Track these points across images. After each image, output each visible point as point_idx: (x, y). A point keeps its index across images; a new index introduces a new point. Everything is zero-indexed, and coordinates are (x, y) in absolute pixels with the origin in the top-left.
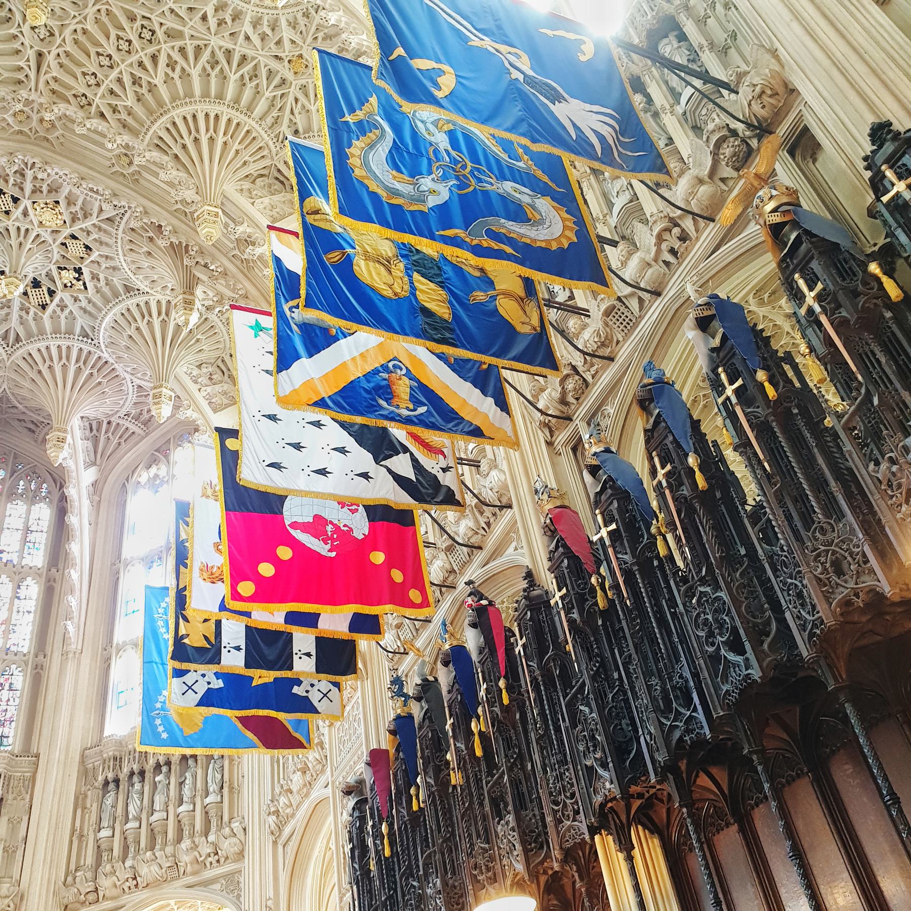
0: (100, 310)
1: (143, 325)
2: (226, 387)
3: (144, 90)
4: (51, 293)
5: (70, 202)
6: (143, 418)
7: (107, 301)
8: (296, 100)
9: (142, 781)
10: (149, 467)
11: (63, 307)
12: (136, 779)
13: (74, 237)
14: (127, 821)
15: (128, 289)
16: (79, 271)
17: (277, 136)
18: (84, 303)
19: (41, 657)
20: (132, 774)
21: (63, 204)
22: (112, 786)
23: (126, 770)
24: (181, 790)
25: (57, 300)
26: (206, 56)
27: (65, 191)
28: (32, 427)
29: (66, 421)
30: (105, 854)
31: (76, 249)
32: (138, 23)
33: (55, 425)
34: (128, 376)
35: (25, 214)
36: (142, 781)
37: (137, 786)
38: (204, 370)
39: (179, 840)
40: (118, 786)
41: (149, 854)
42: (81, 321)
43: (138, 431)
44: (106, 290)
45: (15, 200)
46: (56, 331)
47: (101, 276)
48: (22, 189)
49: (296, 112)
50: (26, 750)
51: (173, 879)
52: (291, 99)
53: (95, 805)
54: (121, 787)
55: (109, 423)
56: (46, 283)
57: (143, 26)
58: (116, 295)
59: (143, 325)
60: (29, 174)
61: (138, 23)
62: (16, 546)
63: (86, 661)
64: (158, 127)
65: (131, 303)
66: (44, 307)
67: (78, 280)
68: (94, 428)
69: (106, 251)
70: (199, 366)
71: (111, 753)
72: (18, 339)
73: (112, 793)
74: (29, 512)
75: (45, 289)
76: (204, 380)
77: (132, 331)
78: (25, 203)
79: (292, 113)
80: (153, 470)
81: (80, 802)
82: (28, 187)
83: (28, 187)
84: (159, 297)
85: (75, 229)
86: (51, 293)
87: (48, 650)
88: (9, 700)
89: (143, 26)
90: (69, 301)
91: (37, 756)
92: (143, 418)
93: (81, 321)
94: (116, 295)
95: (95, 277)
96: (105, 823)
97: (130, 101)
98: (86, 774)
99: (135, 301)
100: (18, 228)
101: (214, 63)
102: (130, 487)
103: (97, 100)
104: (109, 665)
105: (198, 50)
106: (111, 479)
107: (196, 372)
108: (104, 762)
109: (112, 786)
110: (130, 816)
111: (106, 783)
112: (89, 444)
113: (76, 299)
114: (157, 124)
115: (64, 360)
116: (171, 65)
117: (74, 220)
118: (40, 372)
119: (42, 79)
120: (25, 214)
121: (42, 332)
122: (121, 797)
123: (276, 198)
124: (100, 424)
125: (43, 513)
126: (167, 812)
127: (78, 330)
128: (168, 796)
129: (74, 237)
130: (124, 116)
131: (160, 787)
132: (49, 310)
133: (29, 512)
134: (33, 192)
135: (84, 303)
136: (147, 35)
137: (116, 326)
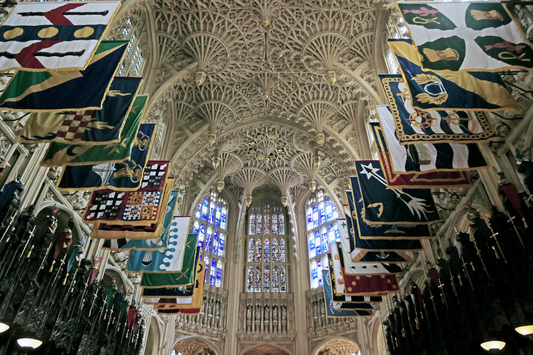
1: (303, 161)
2: (331, 174)
3: (296, 101)
4: (276, 156)
5: (278, 132)
7: (292, 156)
8: (341, 92)
10: (310, 199)
11: (280, 159)
12: (322, 302)
15: (298, 152)
16: (283, 149)
17: (337, 104)
18: (286, 157)
20: (320, 300)
21: (276, 133)
22: (315, 304)
23: (319, 299)
25: (278, 158)
29: (285, 192)
31: (281, 144)
33: (283, 194)
34: (301, 175)
37: (323, 304)
38: (323, 170)
41: (329, 325)
42: (286, 162)
43: (305, 188)
44: (292, 153)
46: (279, 166)
47: (290, 150)
49: (342, 95)
50: (290, 292)
51: (337, 333)
52: (339, 92)
55: (297, 187)
56: (274, 154)
58: (295, 154)
59: (303, 161)
60: (267, 128)
61: (292, 84)
62: (276, 229)
63: (302, 264)
64: (301, 111)
65: (299, 156)
66: (274, 160)
67: (283, 151)
68: (292, 190)
70: (321, 169)
73: (316, 306)
74: (278, 217)
76: (324, 174)
77: (300, 163)
79: (340, 96)
80: (312, 200)
81: (307, 308)
84: (307, 152)
86: (276, 156)
87: (291, 261)
90: (281, 157)
91: (293, 293)
93: (286, 162)
94: (295, 154)
95: (288, 150)
96: (315, 315)
97: (292, 105)
100: (265, 142)
101: (314, 89)
102: (306, 207)
106: (300, 205)
107: (321, 171)
109: (315, 304)
111: (314, 302)
112: (292, 195)
113: (283, 156)
115: (282, 174)
116: (302, 92)
117: (280, 136)
118: (276, 178)
121: (275, 167)
122: (319, 308)
123: (339, 122)
124: (294, 188)
125: (282, 217)
127: (285, 165)
129: (280, 141)
130: (291, 109)
132: (276, 161)
133: (278, 217)
135: (286, 157)
136: (294, 86)
137: (295, 163)
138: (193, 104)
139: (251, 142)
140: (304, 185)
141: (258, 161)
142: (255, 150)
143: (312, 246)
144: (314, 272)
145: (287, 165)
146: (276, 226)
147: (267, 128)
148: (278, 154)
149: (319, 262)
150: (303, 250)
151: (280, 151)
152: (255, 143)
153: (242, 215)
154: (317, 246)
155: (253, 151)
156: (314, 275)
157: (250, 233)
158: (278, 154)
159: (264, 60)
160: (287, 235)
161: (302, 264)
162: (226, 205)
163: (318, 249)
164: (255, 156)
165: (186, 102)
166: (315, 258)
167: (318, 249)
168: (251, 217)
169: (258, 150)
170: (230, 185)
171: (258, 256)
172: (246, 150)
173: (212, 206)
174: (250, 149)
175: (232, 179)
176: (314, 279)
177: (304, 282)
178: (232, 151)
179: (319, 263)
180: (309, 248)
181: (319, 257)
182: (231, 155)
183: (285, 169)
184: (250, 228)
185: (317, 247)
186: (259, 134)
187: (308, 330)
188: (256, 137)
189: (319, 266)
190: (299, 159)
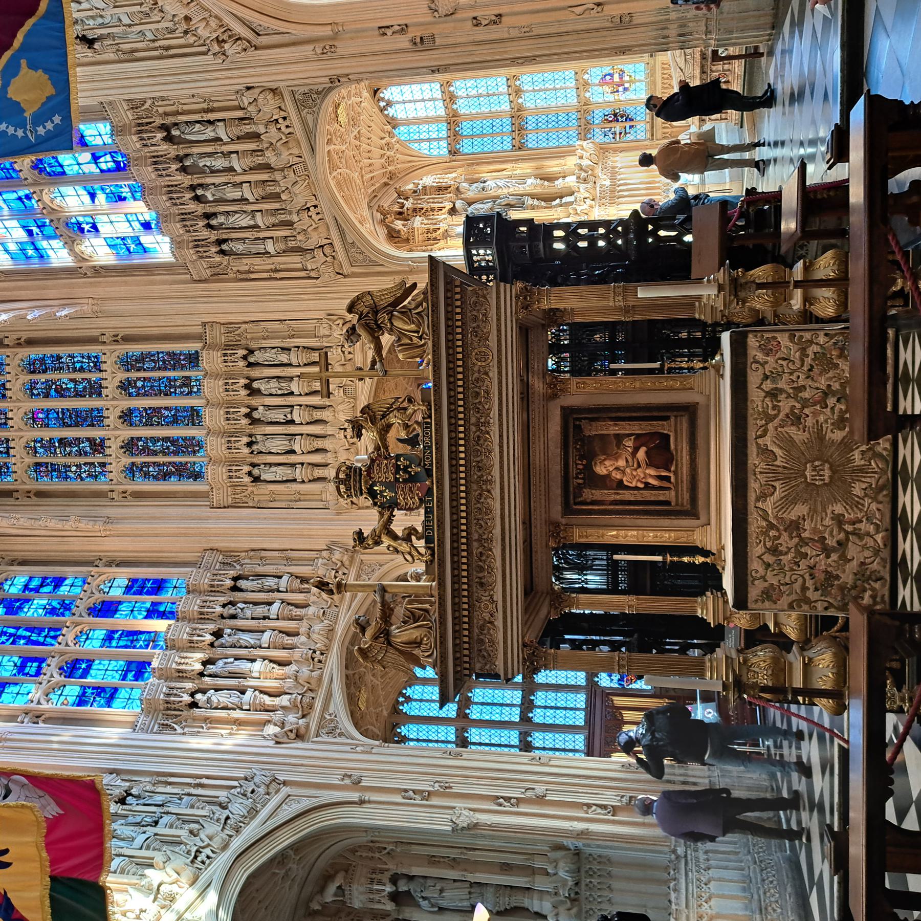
9: (214, 215)
12: (214, 222)
14: (256, 226)
20: (209, 226)
22: (225, 247)
23: (205, 233)
24: (218, 171)
30: (291, 244)
36: (214, 215)
37: (221, 219)
39: (267, 167)
40: (225, 241)
41: (283, 197)
51: (306, 169)
53: (245, 261)
54: (225, 236)
63: (100, 292)
71: (192, 251)
73: (231, 244)
81: (245, 277)
88: (153, 361)
91: (204, 324)
96: (261, 248)
98: (217, 276)
104: (102, 267)
108: (202, 257)
109: (225, 247)
110: (252, 223)
111: (222, 252)
122: (234, 236)
126: (242, 183)
128: (226, 184)
131: (219, 195)
143: (30, 252)
144: (124, 251)
149: (82, 230)
150: (54, 289)
154: (22, 235)
156: (132, 247)
161: (100, 292)
163: (36, 230)
166: (70, 244)
167: (36, 230)
171: (88, 449)
176: (145, 250)
177: (159, 287)
179: (87, 227)
180: (35, 265)
181: (63, 229)
185: (30, 233)
187: (313, 274)
189: (94, 227)
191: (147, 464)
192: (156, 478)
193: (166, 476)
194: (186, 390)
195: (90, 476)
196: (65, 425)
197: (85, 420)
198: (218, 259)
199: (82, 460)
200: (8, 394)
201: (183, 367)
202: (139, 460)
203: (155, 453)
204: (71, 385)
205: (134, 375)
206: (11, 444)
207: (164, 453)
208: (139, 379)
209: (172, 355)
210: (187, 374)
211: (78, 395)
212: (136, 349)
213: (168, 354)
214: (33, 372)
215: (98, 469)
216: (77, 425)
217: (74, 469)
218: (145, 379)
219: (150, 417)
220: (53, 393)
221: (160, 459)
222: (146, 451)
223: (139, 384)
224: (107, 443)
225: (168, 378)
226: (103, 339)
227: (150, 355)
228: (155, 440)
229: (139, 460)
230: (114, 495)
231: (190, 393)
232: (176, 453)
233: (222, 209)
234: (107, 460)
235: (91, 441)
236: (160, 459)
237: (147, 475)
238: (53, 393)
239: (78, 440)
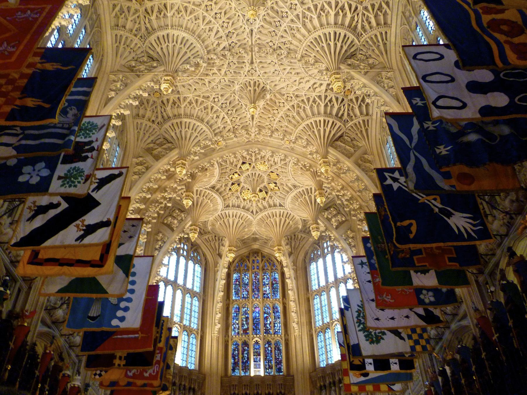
0: (286, 196)
4: (266, 193)
6: (307, 231)
7: (288, 192)
13: (272, 172)
15: (295, 186)
16: (275, 183)
18: (279, 194)
19: (286, 336)
25: (269, 195)
26: (311, 100)
27: (266, 158)
28: (266, 241)
31: (273, 176)
32: (286, 96)
35: (254, 167)
45: (250, 164)
48: (251, 160)
55: (295, 235)
57: (288, 96)
58: (291, 189)
60: (253, 154)
61: (286, 96)
67: (276, 186)
69: (284, 174)
72: (257, 212)
75: (264, 192)
78: (253, 164)
82: (253, 159)
83: (253, 159)
85: (272, 170)
89: (288, 96)
92: (307, 231)
99: (298, 191)
103: (275, 126)
105: (308, 99)
114: (298, 129)
119: (255, 123)
120: (254, 167)
129: (272, 172)
132: (266, 200)
134: (256, 160)
135: (279, 194)
138: (158, 123)
139: (233, 175)
140: (304, 232)
141: (242, 201)
142: (239, 185)
145: (280, 205)
146: (268, 288)
147: (253, 154)
148: (269, 190)
151: (272, 186)
152: (239, 175)
153: (222, 272)
155: (236, 187)
157: (234, 298)
158: (269, 190)
159: (248, 65)
160: (283, 299)
162: (201, 260)
164: (239, 193)
165: (149, 120)
168: (235, 276)
169: (242, 185)
170: (206, 233)
172: (226, 185)
173: (182, 260)
174: (233, 184)
175: (209, 224)
178: (208, 187)
182: (208, 191)
183: (277, 210)
184: (233, 291)
186: (244, 163)
188: (240, 167)
190: (296, 198)
191: (238, 351)
192: (233, 354)
193: (234, 357)
194: (267, 367)
195: (234, 328)
196: (254, 320)
197: (256, 327)
198: (318, 385)
199: (240, 325)
200: (265, 299)
201: (276, 366)
202: (240, 348)
203: (243, 354)
204: (268, 322)
205: (273, 346)
206: (247, 300)
207: (243, 357)
208: (271, 348)
209: (281, 362)
210: (274, 368)
211: (265, 325)
212: (283, 348)
213: (281, 360)
214: (273, 308)
215: (237, 331)
216: (254, 324)
217: (237, 322)
218: (271, 351)
219: (257, 352)
220: (266, 315)
221: (240, 356)
222: (244, 350)
223: (270, 349)
224: (247, 336)
225: (271, 360)
226: (286, 336)
227: (281, 353)
228: (248, 354)
229: (240, 348)
230: (227, 337)
231: (266, 369)
232: (243, 362)
233: (337, 389)
234: (240, 336)
235: (248, 329)
236: (240, 356)
237: (234, 350)
238: (266, 315)
239: (248, 324)
